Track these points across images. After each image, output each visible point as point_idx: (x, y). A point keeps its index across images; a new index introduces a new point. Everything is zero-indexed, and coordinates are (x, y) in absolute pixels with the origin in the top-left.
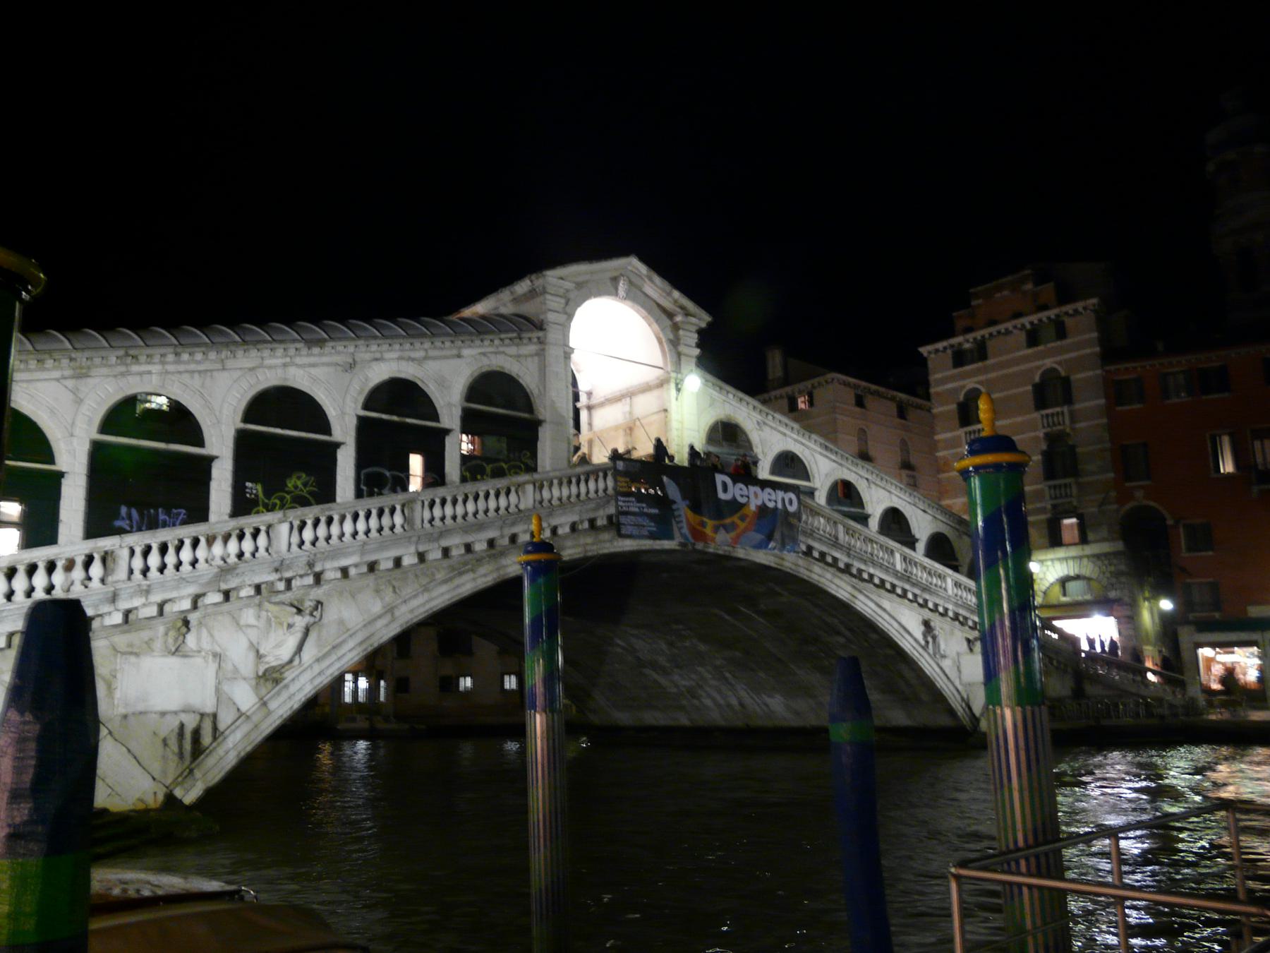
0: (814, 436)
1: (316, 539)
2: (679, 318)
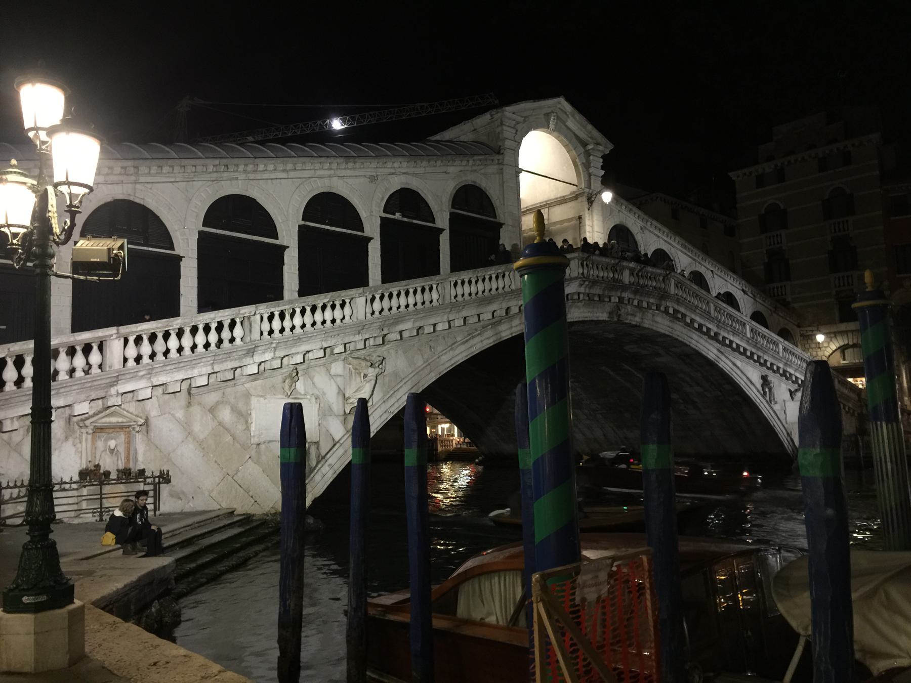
0: (678, 239)
1: (382, 310)
2: (590, 147)
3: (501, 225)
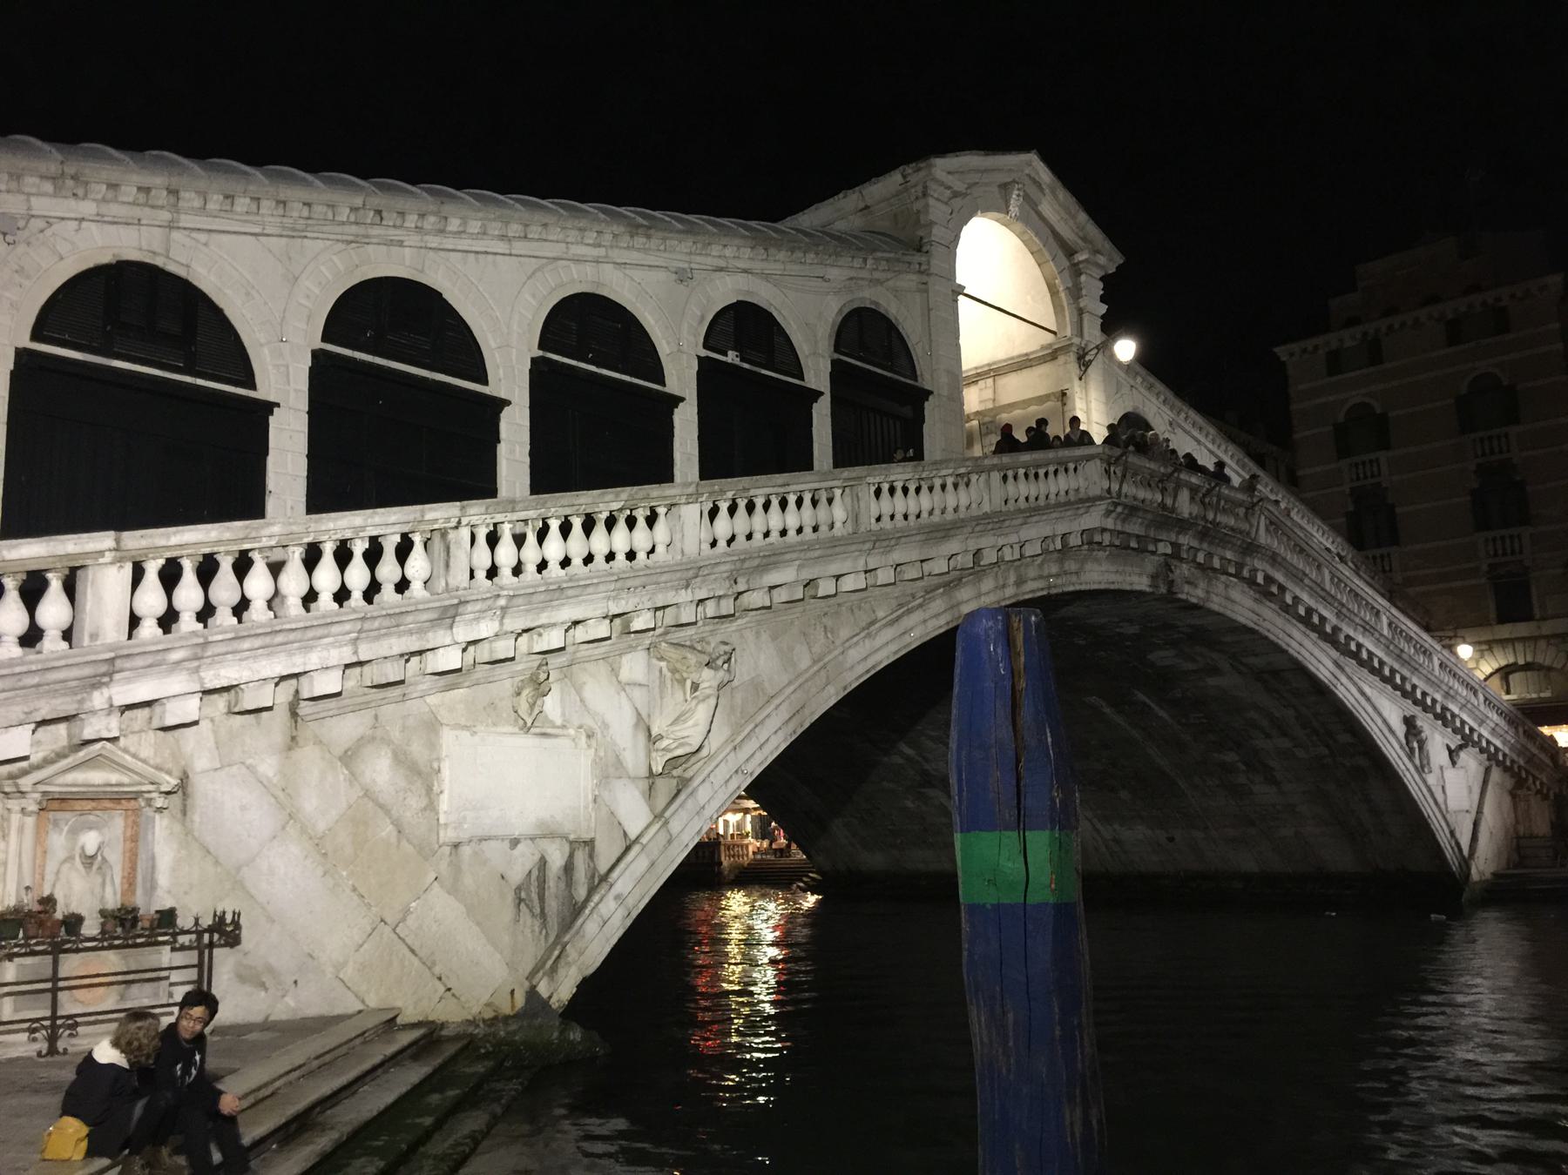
1: (733, 538)
2: (1081, 257)
3: (927, 394)
